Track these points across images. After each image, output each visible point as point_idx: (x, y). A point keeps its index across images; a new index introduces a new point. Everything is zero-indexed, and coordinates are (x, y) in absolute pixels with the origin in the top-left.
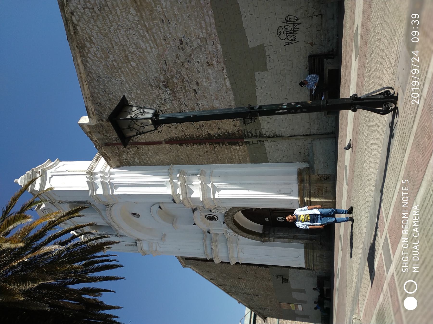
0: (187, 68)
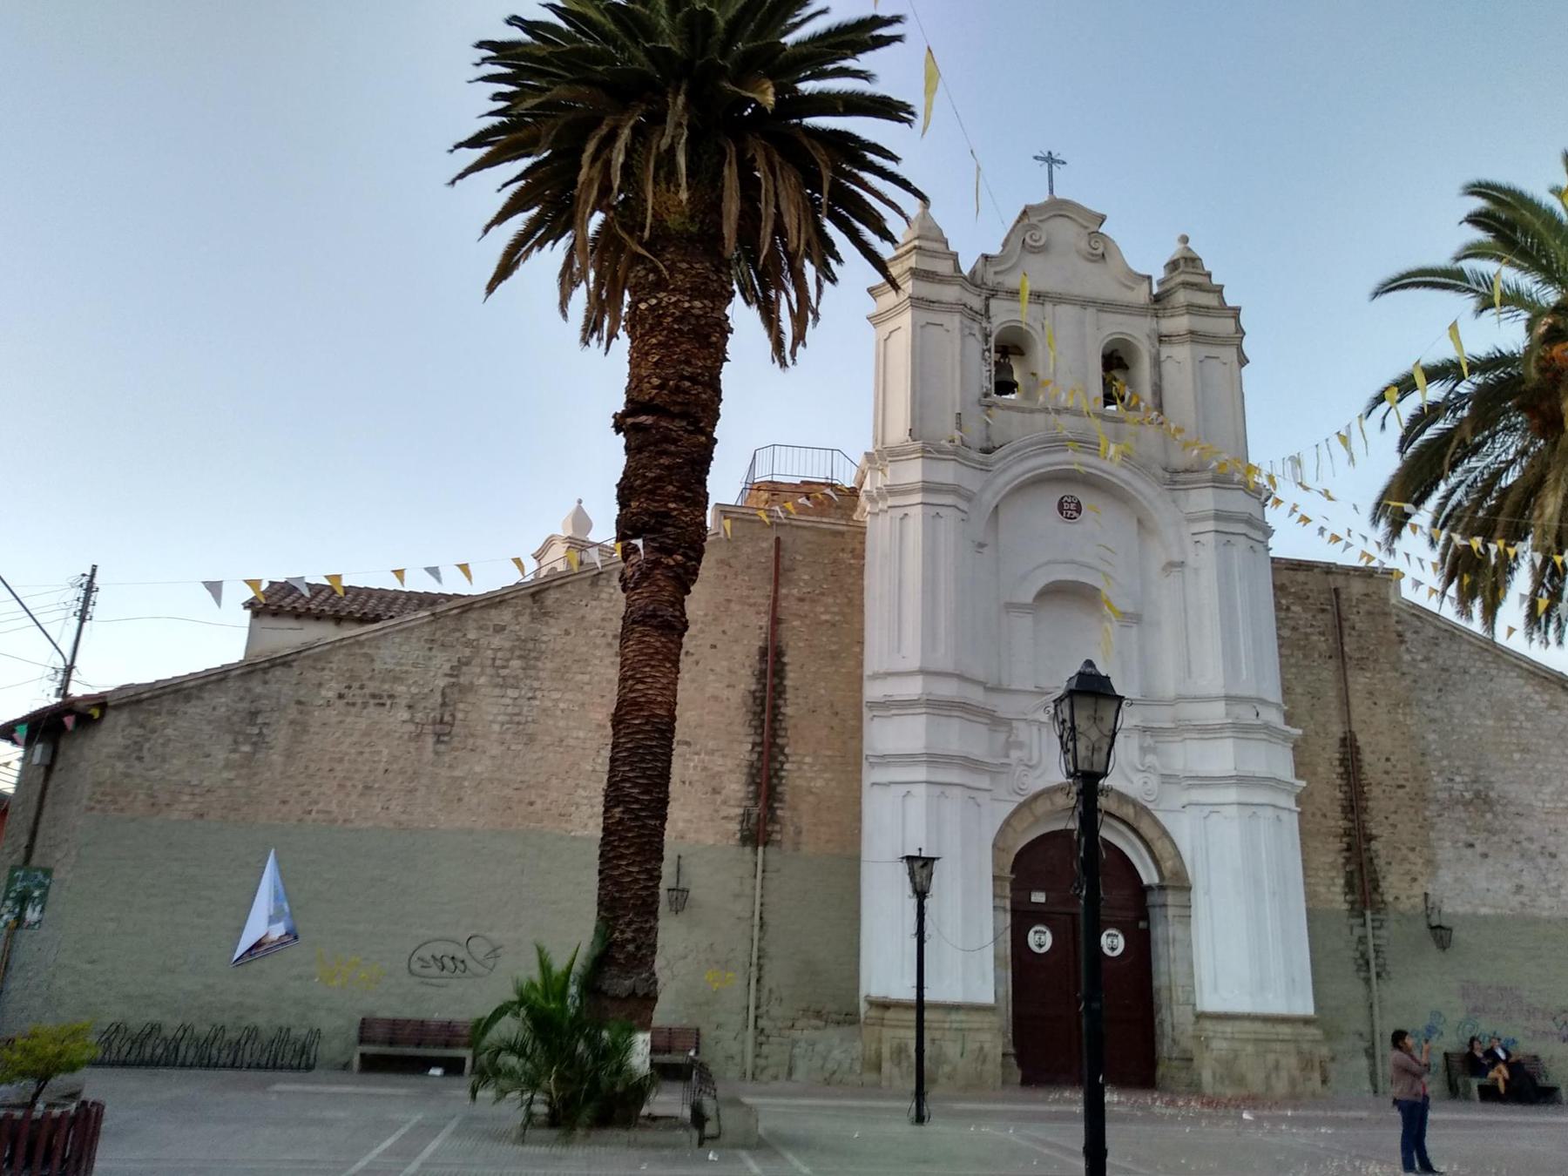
0: (1510, 847)
